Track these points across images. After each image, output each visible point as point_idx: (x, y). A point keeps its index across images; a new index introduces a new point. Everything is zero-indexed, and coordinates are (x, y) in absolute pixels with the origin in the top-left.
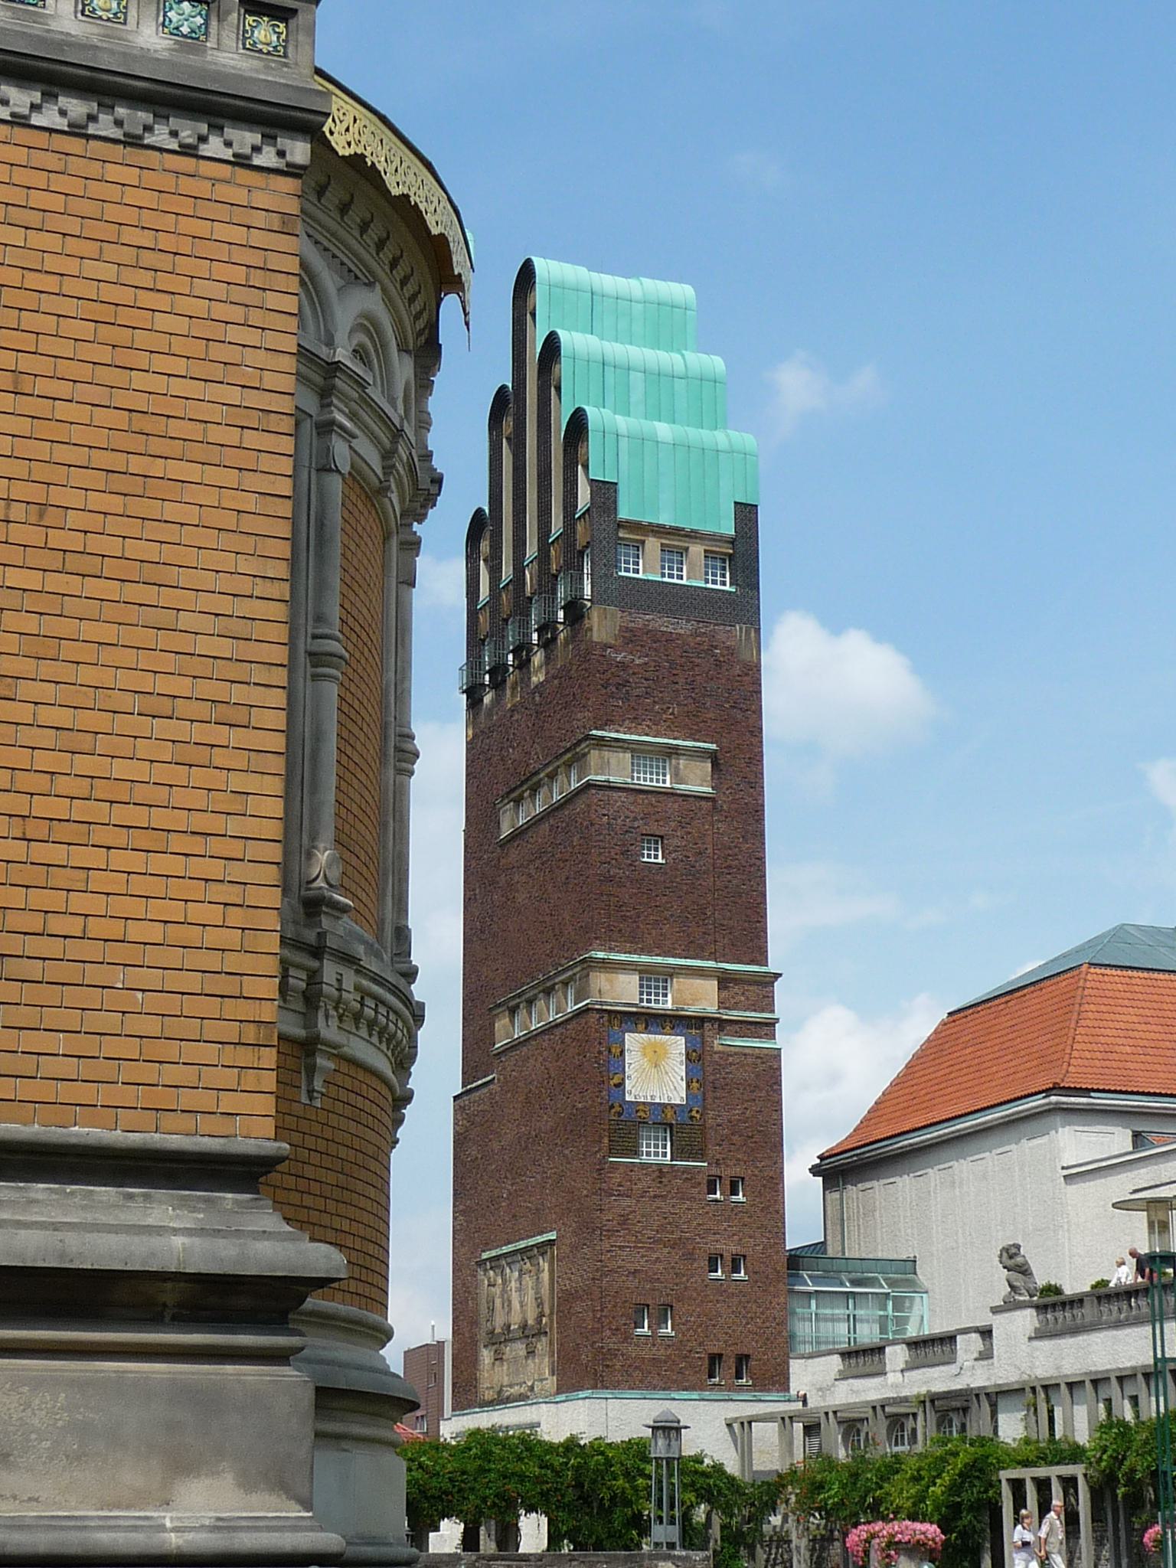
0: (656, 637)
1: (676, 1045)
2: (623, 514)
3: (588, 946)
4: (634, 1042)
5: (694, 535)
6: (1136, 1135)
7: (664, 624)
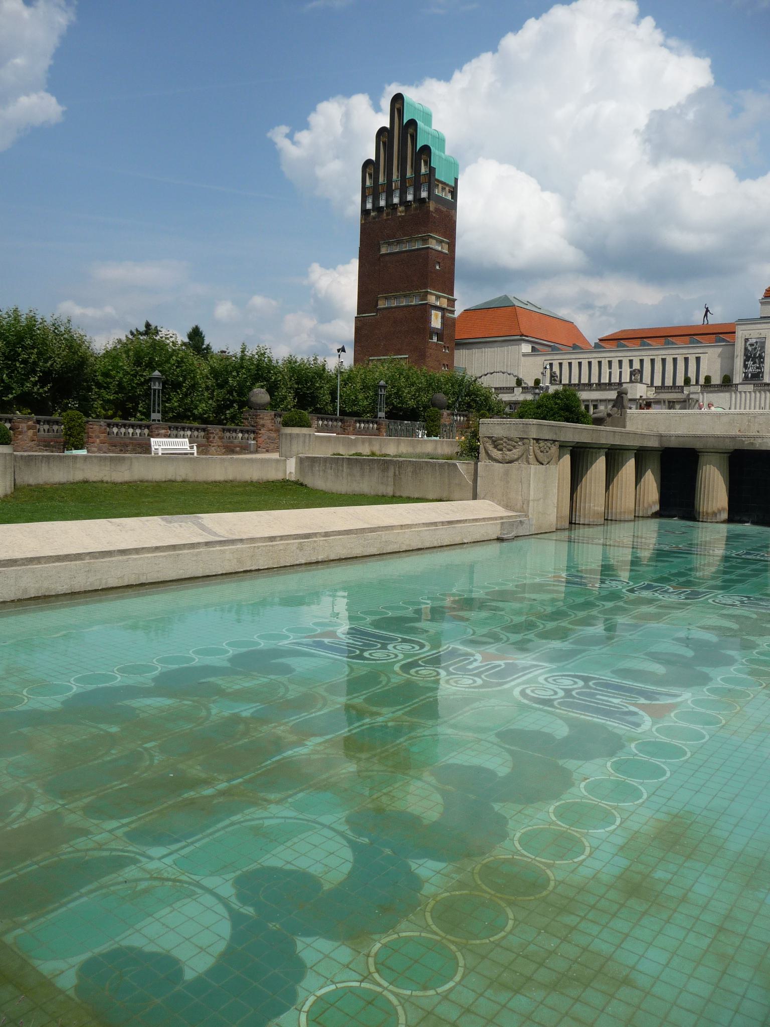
0: (441, 212)
1: (440, 314)
2: (437, 177)
3: (426, 287)
4: (433, 312)
6: (532, 347)
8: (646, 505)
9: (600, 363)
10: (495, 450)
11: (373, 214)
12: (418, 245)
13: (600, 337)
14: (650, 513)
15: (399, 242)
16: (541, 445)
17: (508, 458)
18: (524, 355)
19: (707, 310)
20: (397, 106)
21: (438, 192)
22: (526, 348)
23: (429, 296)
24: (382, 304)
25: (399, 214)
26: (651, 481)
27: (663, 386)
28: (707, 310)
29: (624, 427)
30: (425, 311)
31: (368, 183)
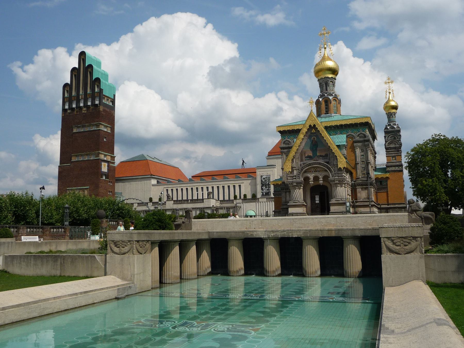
1: (106, 164)
2: (104, 94)
3: (99, 150)
4: (103, 163)
5: (110, 98)
7: (107, 109)
8: (204, 269)
9: (192, 189)
10: (116, 248)
11: (69, 111)
12: (94, 128)
13: (192, 175)
14: (206, 273)
15: (83, 127)
16: (140, 244)
17: (122, 252)
18: (153, 185)
19: (243, 162)
20: (82, 57)
21: (104, 101)
22: (154, 182)
23: (100, 155)
24: (74, 159)
25: (83, 112)
26: (206, 257)
27: (224, 200)
28: (243, 162)
29: (191, 229)
30: (98, 162)
31: (66, 95)
